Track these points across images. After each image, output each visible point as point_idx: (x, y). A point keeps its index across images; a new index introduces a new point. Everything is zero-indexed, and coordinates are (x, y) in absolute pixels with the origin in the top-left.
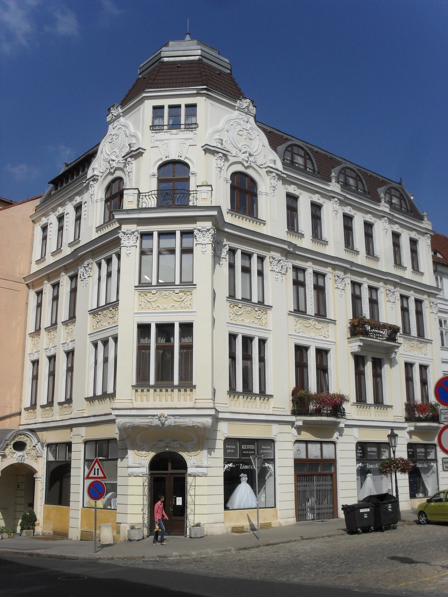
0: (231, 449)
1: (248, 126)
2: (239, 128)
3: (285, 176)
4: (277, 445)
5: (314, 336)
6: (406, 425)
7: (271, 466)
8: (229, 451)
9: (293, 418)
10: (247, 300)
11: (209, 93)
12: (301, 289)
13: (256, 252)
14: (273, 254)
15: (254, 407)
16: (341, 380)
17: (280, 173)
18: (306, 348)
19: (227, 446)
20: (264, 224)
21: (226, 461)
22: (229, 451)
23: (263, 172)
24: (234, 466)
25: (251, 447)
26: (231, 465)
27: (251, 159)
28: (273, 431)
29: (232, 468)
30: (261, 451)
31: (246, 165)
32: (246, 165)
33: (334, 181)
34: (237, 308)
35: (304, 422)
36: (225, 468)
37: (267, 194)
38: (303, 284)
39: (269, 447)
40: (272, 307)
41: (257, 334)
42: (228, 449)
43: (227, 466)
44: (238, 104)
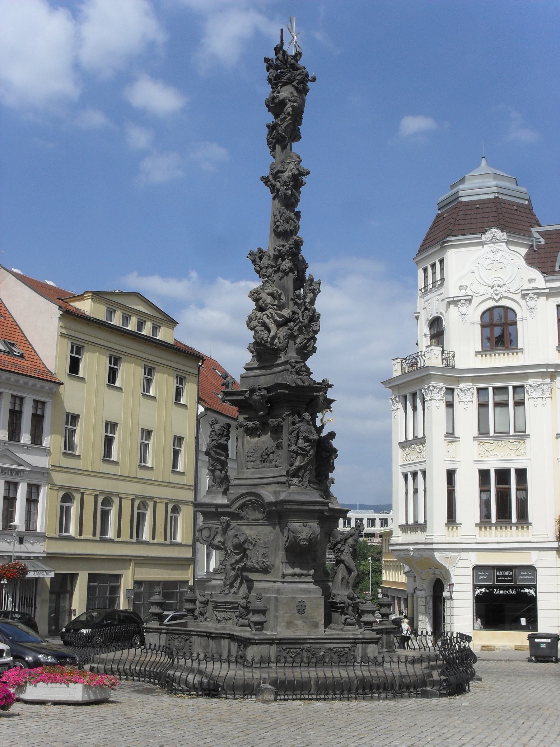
0: (484, 575)
1: (500, 254)
2: (489, 261)
4: (539, 572)
7: (532, 592)
8: (482, 577)
10: (502, 435)
15: (511, 535)
17: (538, 291)
19: (479, 573)
20: (522, 352)
21: (476, 586)
22: (482, 577)
24: (487, 591)
25: (509, 573)
26: (483, 590)
27: (504, 288)
29: (484, 593)
30: (520, 577)
32: (497, 298)
36: (477, 593)
39: (530, 574)
40: (529, 435)
41: (512, 466)
42: (481, 575)
43: (478, 591)
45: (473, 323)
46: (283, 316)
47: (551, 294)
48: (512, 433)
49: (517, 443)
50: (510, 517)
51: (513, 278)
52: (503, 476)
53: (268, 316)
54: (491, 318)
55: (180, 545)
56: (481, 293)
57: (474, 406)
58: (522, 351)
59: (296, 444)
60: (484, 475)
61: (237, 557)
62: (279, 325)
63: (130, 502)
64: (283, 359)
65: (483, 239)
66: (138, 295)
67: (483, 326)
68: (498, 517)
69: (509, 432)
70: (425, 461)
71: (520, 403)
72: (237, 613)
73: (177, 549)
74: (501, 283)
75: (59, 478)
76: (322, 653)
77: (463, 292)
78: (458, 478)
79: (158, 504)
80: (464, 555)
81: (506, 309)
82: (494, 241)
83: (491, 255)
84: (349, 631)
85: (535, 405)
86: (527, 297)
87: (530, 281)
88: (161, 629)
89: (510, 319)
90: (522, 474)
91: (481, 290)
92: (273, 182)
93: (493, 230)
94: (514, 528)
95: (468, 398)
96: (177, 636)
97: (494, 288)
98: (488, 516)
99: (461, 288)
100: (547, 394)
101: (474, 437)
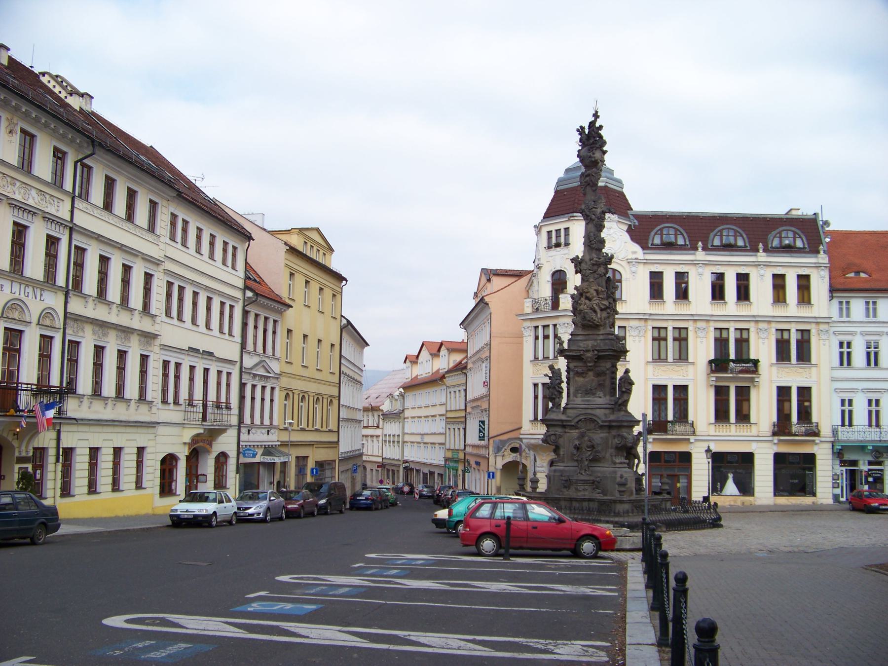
1: (612, 231)
5: (671, 376)
6: (771, 438)
12: (663, 343)
14: (633, 323)
16: (701, 405)
18: (665, 387)
23: (624, 263)
33: (700, 249)
35: (654, 439)
37: (626, 280)
38: (665, 339)
47: (646, 263)
55: (330, 431)
58: (625, 301)
62: (602, 310)
66: (317, 230)
75: (285, 382)
87: (635, 253)
92: (588, 213)
100: (641, 334)
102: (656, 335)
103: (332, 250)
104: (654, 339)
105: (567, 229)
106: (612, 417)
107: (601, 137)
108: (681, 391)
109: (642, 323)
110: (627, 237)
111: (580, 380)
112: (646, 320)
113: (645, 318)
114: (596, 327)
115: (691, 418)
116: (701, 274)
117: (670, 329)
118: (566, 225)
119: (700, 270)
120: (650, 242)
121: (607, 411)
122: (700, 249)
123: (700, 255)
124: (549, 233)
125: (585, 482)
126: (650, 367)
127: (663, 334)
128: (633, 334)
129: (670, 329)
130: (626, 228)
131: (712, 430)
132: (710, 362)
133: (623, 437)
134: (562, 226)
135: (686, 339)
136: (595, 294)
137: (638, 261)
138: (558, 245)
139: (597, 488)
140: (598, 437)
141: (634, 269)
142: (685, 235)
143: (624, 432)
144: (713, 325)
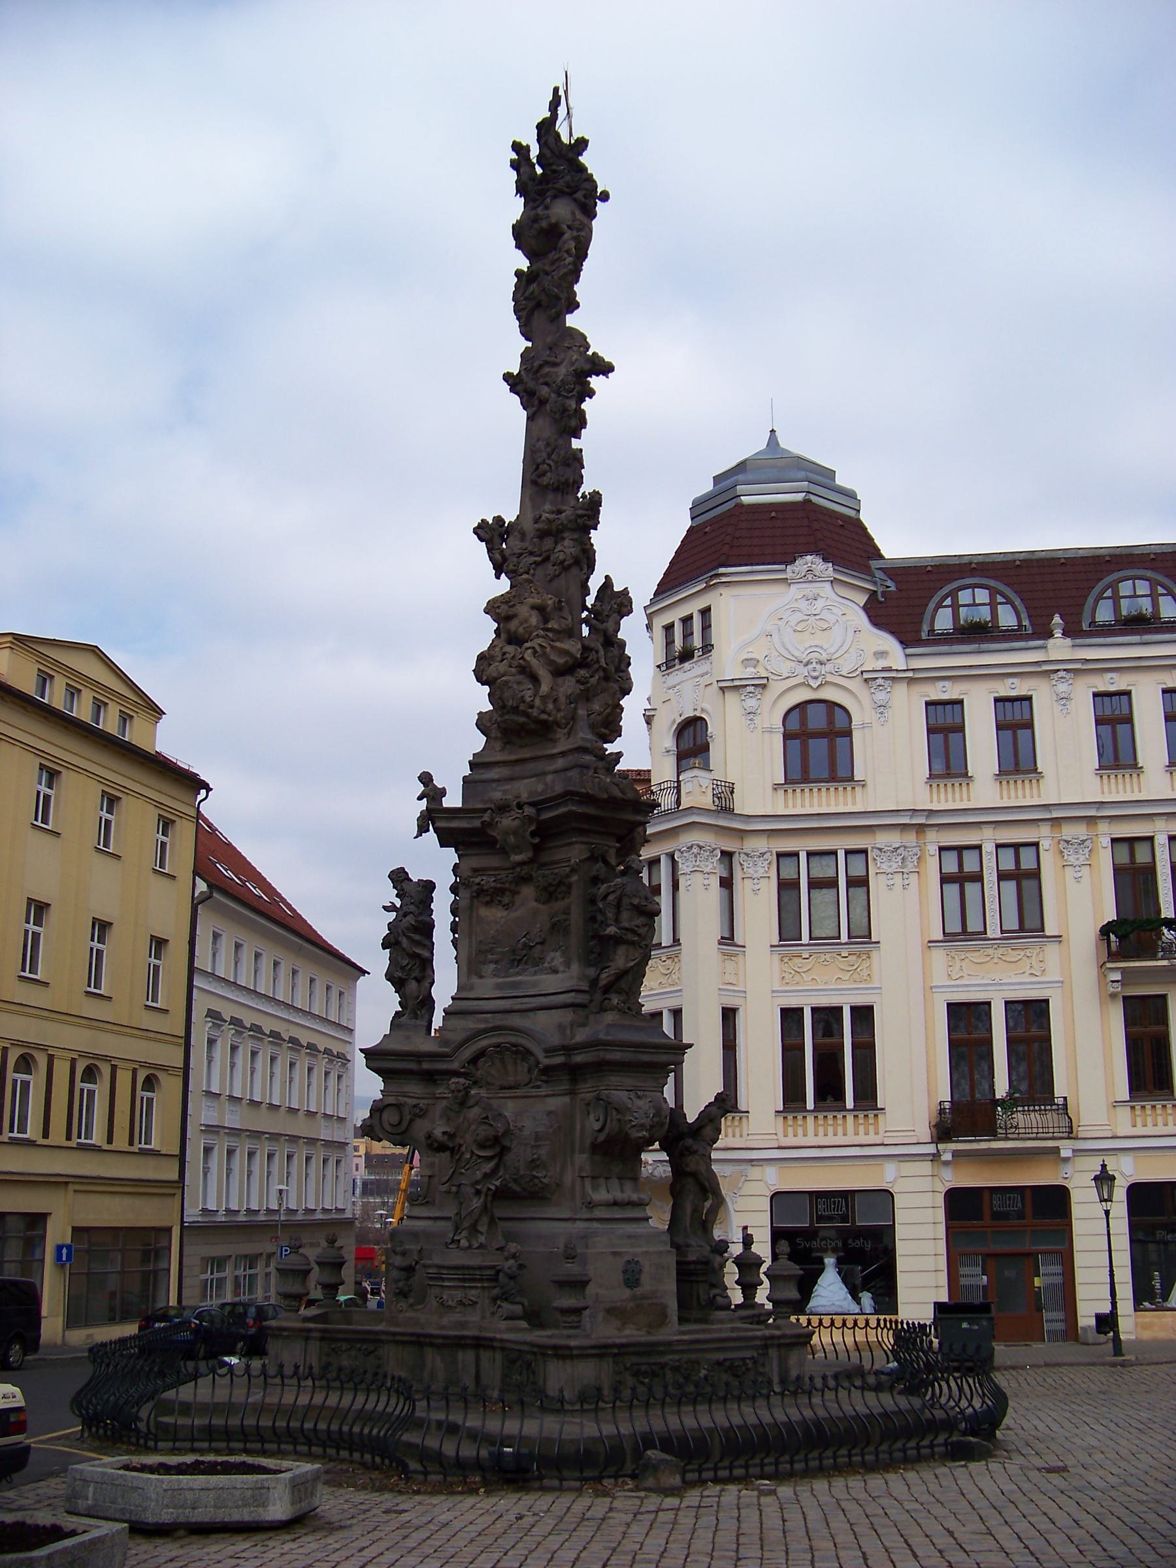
1: (820, 604)
2: (799, 616)
3: (910, 674)
5: (997, 978)
9: (931, 1149)
11: (724, 579)
12: (971, 889)
13: (840, 844)
14: (884, 839)
15: (843, 1131)
18: (981, 1010)
23: (855, 685)
28: (886, 1176)
31: (815, 686)
33: (1058, 633)
34: (800, 960)
35: (956, 1154)
37: (863, 726)
38: (978, 878)
41: (846, 1001)
44: (791, 571)
45: (771, 731)
46: (567, 653)
47: (913, 679)
48: (844, 938)
49: (854, 957)
50: (841, 1097)
51: (845, 648)
52: (827, 1017)
53: (535, 652)
54: (803, 721)
55: (155, 1154)
56: (785, 675)
57: (770, 889)
58: (863, 784)
59: (617, 921)
60: (790, 1017)
61: (488, 1167)
62: (559, 672)
63: (67, 1065)
64: (563, 745)
65: (789, 575)
67: (787, 736)
68: (820, 1095)
69: (839, 938)
70: (680, 990)
71: (859, 883)
72: (496, 1291)
73: (151, 1162)
74: (824, 657)
76: (703, 1372)
77: (750, 672)
78: (742, 1022)
79: (119, 1072)
80: (754, 1172)
81: (832, 706)
82: (810, 577)
83: (803, 605)
84: (721, 1321)
85: (890, 887)
86: (874, 684)
87: (882, 654)
88: (310, 1330)
89: (840, 723)
90: (864, 1015)
91: (785, 668)
92: (531, 385)
93: (809, 558)
94: (810, 1119)
95: (761, 872)
96: (345, 1346)
97: (810, 667)
98: (840, 1096)
99: (747, 662)
100: (910, 866)
101: (772, 946)
102: (951, 867)
103: (157, 712)
104: (945, 879)
105: (706, 612)
106: (581, 1036)
107: (582, 169)
108: (1031, 1016)
109: (911, 838)
110: (862, 619)
111: (493, 915)
112: (921, 828)
113: (917, 824)
114: (543, 730)
115: (1060, 1090)
116: (1064, 699)
117: (988, 848)
118: (700, 603)
119: (1062, 688)
120: (925, 628)
121: (567, 1016)
122: (1058, 633)
123: (1059, 648)
124: (669, 628)
125: (467, 1275)
126: (939, 956)
127: (970, 865)
128: (885, 867)
129: (988, 848)
130: (862, 599)
131: (1123, 1122)
132: (1106, 930)
133: (608, 1106)
134: (693, 608)
135: (1035, 874)
136: (534, 619)
137: (892, 677)
138: (686, 655)
139: (505, 1297)
140: (531, 1114)
141: (881, 696)
142: (1018, 602)
143: (618, 1089)
144: (1106, 832)
